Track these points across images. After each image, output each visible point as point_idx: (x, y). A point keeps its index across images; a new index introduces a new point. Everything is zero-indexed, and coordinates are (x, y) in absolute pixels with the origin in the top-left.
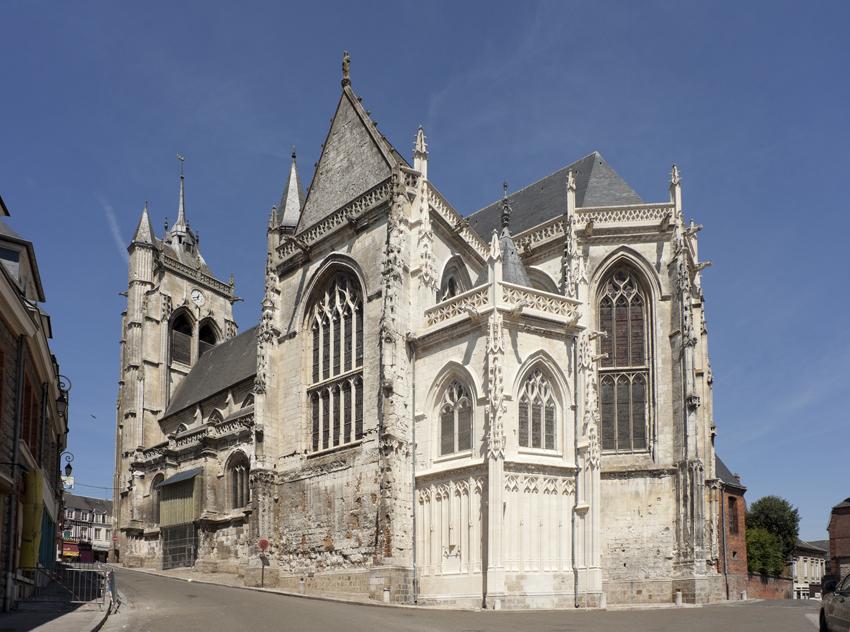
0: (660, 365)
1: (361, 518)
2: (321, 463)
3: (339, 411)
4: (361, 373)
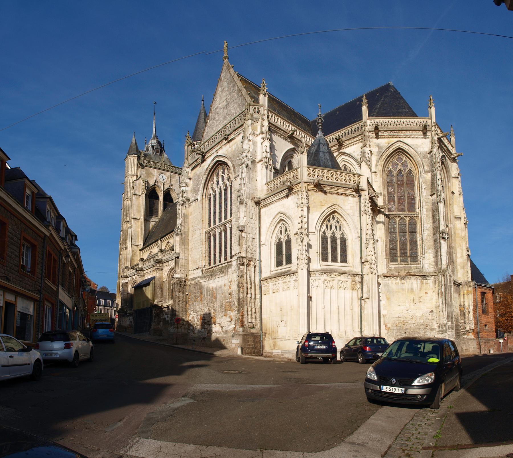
2: (211, 273)
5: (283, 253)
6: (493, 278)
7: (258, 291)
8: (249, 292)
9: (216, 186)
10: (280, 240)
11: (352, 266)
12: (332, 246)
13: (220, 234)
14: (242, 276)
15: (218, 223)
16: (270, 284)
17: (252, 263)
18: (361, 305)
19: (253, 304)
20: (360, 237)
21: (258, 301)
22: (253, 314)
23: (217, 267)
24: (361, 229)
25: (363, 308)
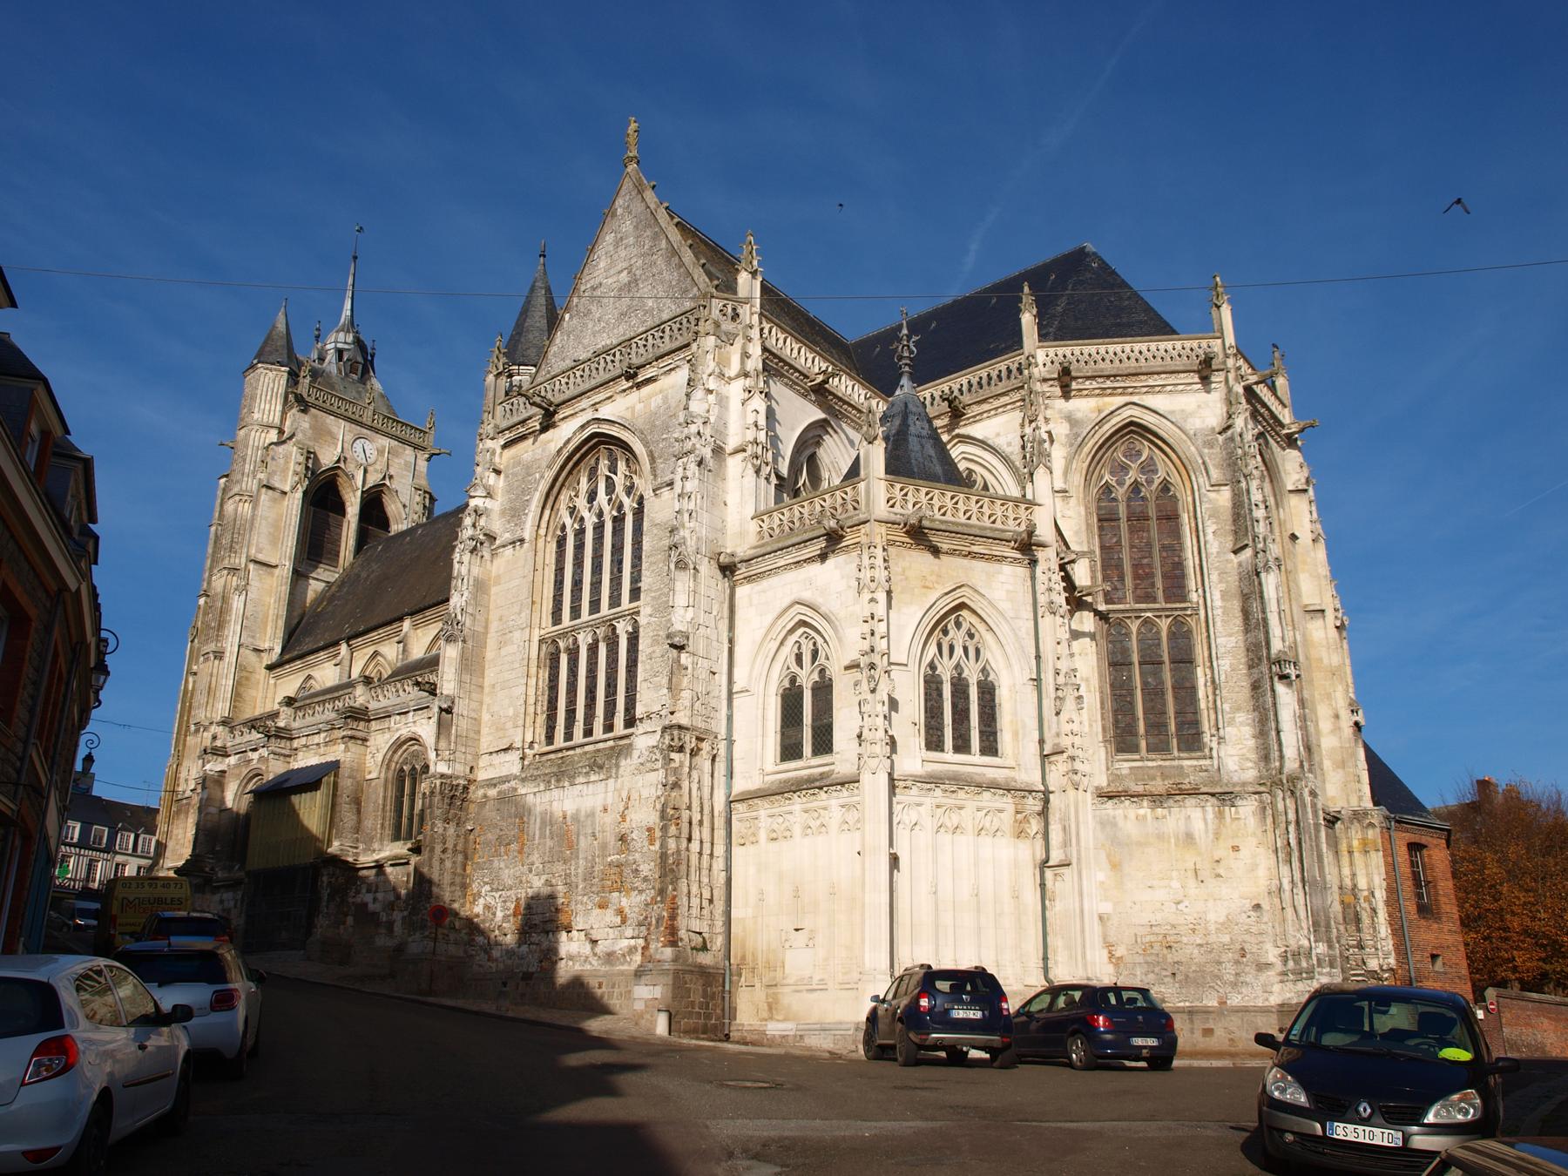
0: (1218, 603)
1: (627, 871)
2: (560, 773)
3: (595, 677)
4: (638, 613)
5: (805, 719)
6: (1440, 790)
7: (720, 834)
8: (696, 835)
9: (585, 505)
10: (793, 680)
11: (1013, 764)
12: (954, 706)
13: (593, 649)
14: (676, 785)
15: (585, 615)
16: (762, 813)
17: (705, 746)
18: (1043, 885)
19: (705, 872)
20: (1037, 681)
21: (719, 864)
22: (705, 904)
23: (578, 751)
24: (1038, 657)
25: (1048, 894)
